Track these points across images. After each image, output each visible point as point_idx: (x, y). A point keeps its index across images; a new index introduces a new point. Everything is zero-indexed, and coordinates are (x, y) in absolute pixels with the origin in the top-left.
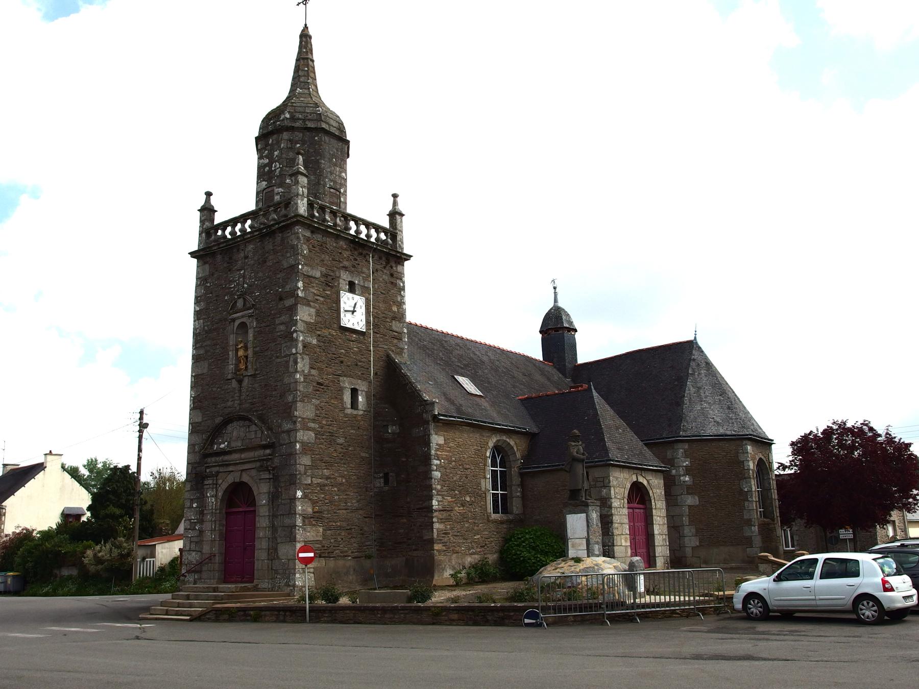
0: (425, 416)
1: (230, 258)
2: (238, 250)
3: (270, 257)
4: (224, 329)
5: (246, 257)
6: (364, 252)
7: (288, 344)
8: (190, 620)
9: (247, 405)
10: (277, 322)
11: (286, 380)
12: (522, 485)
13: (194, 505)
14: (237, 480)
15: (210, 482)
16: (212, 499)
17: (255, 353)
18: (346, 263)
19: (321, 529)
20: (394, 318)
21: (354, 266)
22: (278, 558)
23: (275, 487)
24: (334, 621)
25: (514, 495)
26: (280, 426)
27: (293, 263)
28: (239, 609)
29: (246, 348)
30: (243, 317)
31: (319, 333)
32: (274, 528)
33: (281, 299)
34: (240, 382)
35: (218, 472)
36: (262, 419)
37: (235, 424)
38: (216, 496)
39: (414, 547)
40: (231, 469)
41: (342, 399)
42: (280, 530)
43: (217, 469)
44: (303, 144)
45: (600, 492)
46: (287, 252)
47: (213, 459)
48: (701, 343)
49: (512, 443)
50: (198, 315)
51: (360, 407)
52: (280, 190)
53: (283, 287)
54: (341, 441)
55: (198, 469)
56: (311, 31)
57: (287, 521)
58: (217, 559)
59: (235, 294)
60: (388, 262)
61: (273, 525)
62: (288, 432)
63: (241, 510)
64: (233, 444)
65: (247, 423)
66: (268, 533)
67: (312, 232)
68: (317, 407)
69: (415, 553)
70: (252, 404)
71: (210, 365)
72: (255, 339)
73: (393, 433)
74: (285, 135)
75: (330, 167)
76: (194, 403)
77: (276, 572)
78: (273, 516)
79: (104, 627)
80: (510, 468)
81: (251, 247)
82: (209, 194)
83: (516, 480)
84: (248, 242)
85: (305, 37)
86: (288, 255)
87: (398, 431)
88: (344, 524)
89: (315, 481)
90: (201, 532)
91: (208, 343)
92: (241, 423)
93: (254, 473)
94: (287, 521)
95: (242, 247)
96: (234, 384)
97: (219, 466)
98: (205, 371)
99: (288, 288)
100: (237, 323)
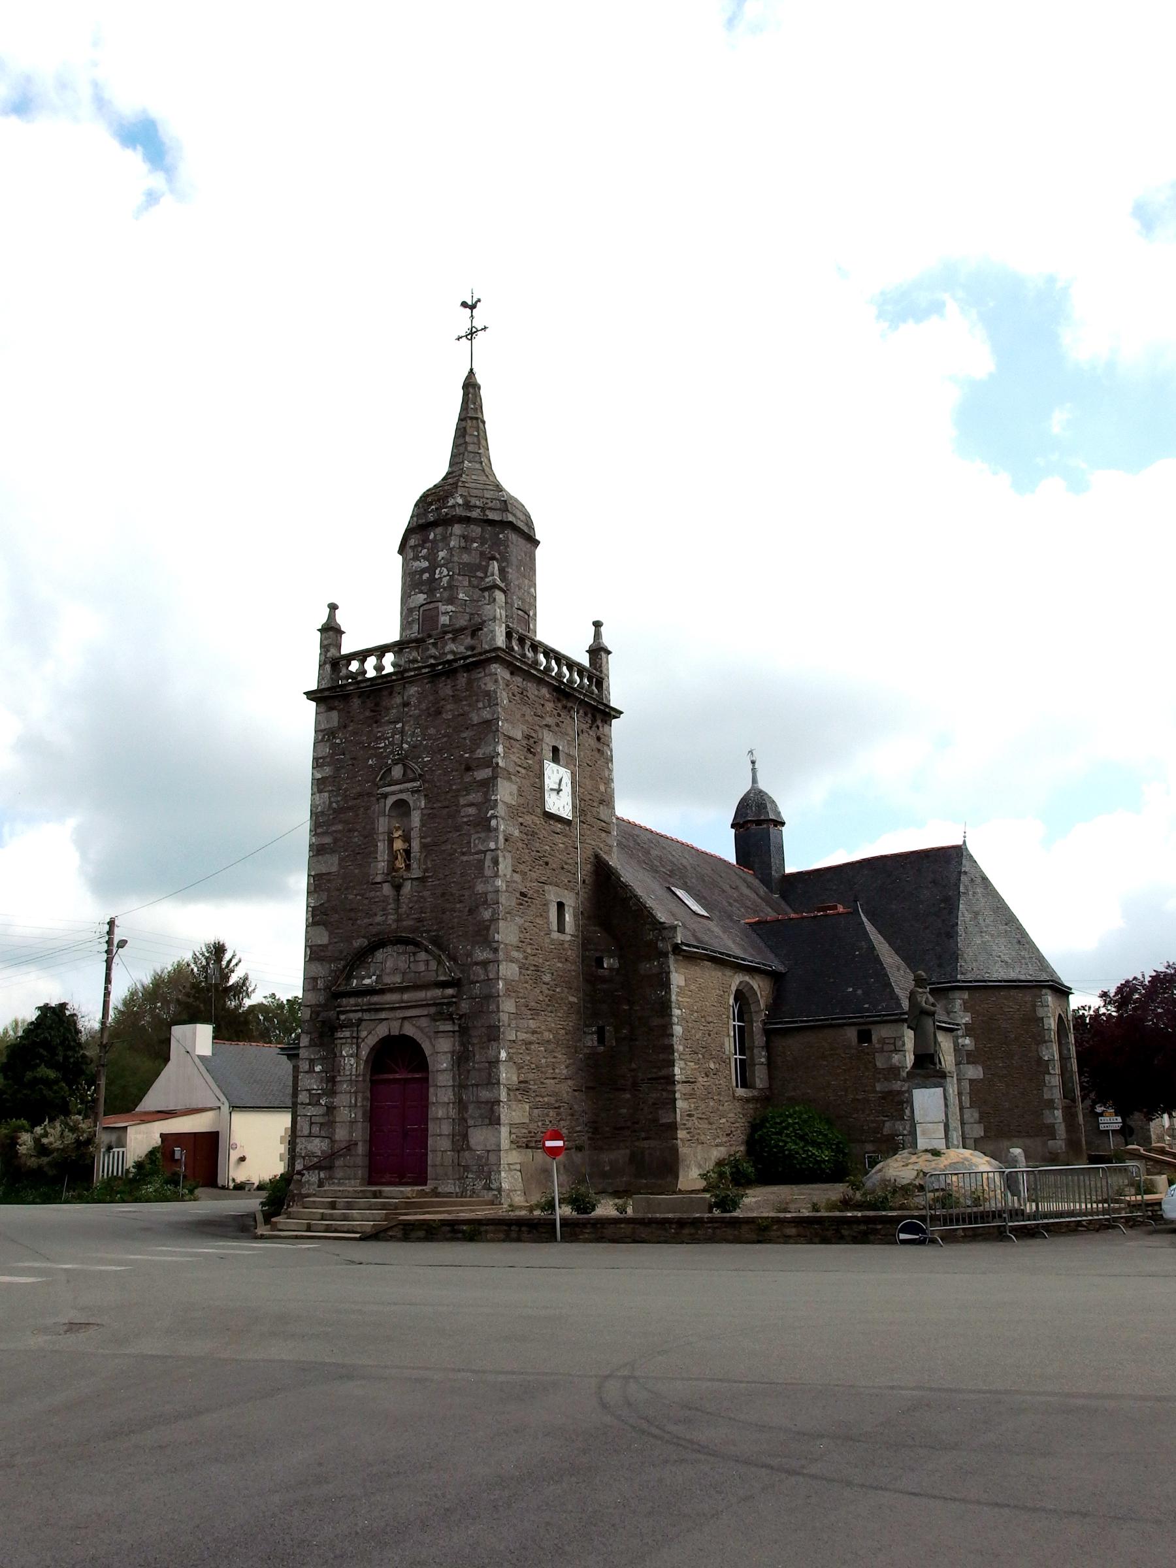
0: (660, 945)
1: (377, 705)
2: (391, 693)
3: (449, 707)
4: (367, 808)
5: (406, 704)
6: (570, 705)
7: (483, 835)
8: (360, 1239)
9: (411, 923)
10: (462, 801)
11: (480, 888)
12: (768, 1047)
13: (318, 1068)
14: (395, 1032)
15: (348, 1034)
16: (352, 1061)
17: (424, 846)
18: (549, 720)
19: (527, 1107)
20: (602, 802)
21: (557, 725)
22: (469, 1148)
23: (462, 1044)
24: (600, 1239)
25: (757, 1061)
26: (469, 954)
27: (489, 717)
28: (444, 1223)
29: (406, 838)
30: (401, 791)
31: (520, 820)
32: (461, 1105)
33: (468, 769)
34: (398, 888)
35: (360, 1020)
36: (436, 941)
37: (389, 949)
38: (357, 1056)
39: (643, 1135)
40: (383, 1015)
41: (547, 918)
42: (471, 1107)
43: (359, 1015)
44: (482, 544)
45: (890, 1058)
46: (477, 701)
47: (352, 1001)
48: (973, 849)
49: (756, 987)
50: (319, 785)
51: (567, 929)
52: (450, 608)
53: (472, 752)
54: (547, 978)
55: (324, 1015)
56: (480, 379)
57: (485, 1094)
58: (361, 1149)
59: (387, 757)
60: (594, 720)
61: (461, 1100)
62: (485, 964)
63: (397, 1076)
64: (387, 980)
65: (411, 948)
66: (453, 1113)
67: (512, 673)
68: (523, 930)
69: (646, 1144)
70: (420, 920)
71: (341, 860)
72: (423, 825)
73: (611, 969)
74: (457, 529)
75: (518, 578)
76: (313, 916)
77: (467, 1168)
78: (460, 1086)
80: (751, 1022)
81: (413, 690)
82: (333, 607)
83: (759, 1039)
84: (410, 682)
85: (471, 387)
86: (480, 705)
87: (617, 966)
88: (552, 1100)
89: (522, 1036)
90: (331, 1109)
91: (340, 827)
92: (401, 948)
93: (424, 1022)
94: (485, 1094)
95: (398, 689)
96: (387, 889)
97: (362, 1011)
98: (334, 869)
99: (480, 753)
100: (390, 800)
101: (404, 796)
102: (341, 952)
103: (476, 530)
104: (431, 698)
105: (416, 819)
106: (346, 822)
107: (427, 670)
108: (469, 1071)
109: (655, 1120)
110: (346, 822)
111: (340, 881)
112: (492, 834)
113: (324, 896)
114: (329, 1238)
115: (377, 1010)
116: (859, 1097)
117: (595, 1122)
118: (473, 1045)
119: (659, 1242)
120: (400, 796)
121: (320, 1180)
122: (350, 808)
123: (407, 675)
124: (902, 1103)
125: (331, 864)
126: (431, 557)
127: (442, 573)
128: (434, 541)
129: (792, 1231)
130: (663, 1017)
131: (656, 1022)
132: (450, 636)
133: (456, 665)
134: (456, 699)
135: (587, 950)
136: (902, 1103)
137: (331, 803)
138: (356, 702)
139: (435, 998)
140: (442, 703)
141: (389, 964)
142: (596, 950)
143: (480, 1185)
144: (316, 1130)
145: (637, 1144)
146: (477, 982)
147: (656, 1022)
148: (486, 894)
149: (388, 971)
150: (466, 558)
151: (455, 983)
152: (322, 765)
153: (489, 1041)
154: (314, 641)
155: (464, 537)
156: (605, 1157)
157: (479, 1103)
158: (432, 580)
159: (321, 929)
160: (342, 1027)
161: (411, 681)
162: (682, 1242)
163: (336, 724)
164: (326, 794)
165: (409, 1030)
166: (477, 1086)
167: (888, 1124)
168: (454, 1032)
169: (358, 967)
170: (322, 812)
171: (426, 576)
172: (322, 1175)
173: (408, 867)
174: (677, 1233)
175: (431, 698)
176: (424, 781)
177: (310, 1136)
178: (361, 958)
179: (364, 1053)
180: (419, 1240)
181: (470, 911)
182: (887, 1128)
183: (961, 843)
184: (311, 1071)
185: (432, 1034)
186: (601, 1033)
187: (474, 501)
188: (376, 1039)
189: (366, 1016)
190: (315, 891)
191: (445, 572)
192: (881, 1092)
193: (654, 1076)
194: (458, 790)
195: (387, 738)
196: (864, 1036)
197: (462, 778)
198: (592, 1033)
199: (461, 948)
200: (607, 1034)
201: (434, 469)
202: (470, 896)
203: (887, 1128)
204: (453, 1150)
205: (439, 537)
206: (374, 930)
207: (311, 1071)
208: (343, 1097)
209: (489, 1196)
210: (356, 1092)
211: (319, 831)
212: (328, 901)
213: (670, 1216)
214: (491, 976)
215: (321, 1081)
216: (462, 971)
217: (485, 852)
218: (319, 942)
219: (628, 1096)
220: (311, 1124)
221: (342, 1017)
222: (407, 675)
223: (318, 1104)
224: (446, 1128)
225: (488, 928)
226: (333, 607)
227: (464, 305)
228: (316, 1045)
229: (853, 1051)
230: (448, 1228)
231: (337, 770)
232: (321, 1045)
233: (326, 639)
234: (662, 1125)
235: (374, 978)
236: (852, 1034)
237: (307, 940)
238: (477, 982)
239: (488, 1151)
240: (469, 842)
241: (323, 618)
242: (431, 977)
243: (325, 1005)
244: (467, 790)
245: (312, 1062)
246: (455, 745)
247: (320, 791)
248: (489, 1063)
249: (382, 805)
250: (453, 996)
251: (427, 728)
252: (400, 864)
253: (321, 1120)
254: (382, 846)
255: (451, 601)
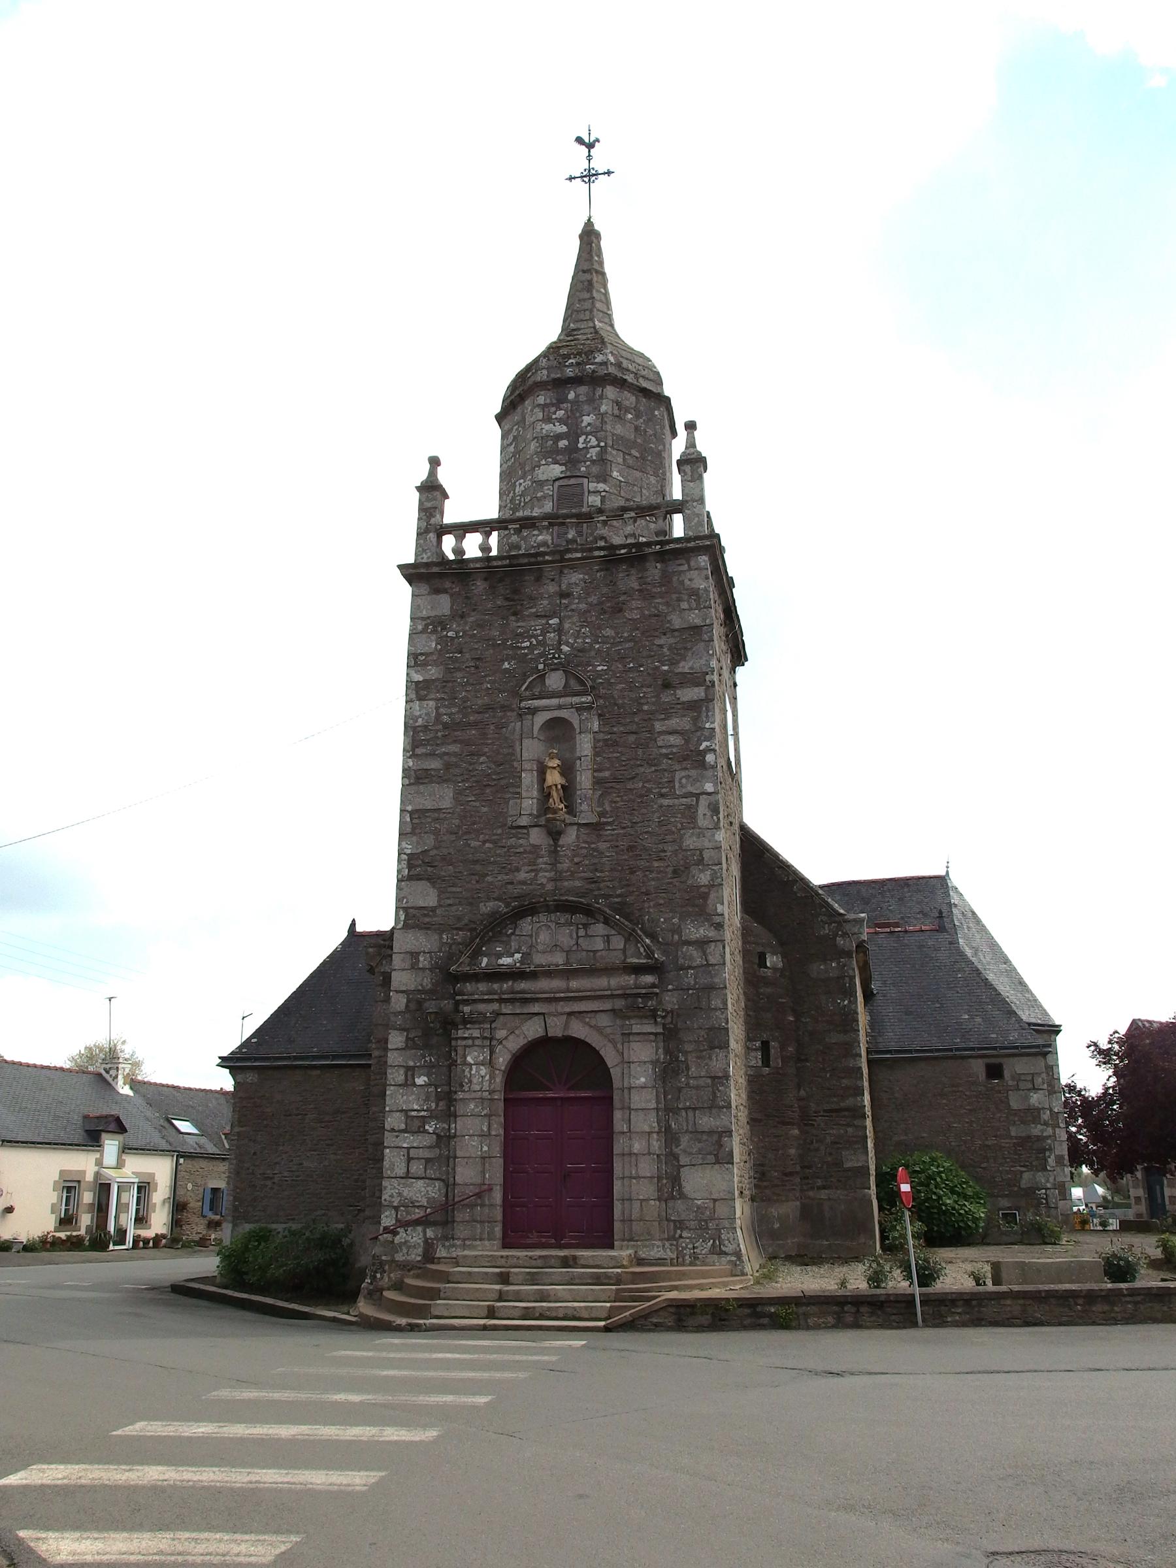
0: (840, 941)
1: (516, 591)
2: (538, 579)
3: (634, 604)
4: (500, 727)
5: (564, 595)
7: (693, 773)
8: (607, 1329)
9: (578, 884)
10: (658, 726)
11: (690, 842)
13: (421, 1080)
14: (556, 1031)
15: (476, 1033)
16: (482, 1071)
17: (597, 782)
22: (682, 1196)
23: (667, 1051)
24: (977, 1322)
26: (678, 930)
27: (698, 622)
28: (743, 1303)
29: (567, 770)
30: (560, 707)
32: (670, 1136)
33: (667, 686)
34: (555, 834)
35: (498, 1014)
36: (620, 909)
37: (543, 917)
38: (491, 1064)
39: (819, 1182)
40: (536, 1008)
42: (685, 1140)
43: (496, 1006)
44: (637, 416)
45: (1027, 1098)
46: (679, 600)
47: (482, 987)
48: (955, 880)
50: (417, 691)
52: (601, 486)
53: (673, 663)
55: (431, 1006)
57: (706, 1121)
58: (498, 1196)
59: (536, 660)
61: (668, 1128)
62: (702, 944)
63: (550, 1095)
64: (540, 959)
65: (580, 918)
66: (656, 1145)
69: (824, 1194)
70: (592, 881)
71: (458, 793)
72: (596, 754)
73: (775, 969)
74: (610, 392)
76: (410, 866)
77: (680, 1225)
78: (668, 1110)
79: (557, 1350)
81: (575, 577)
82: (435, 462)
84: (572, 567)
85: (590, 238)
86: (684, 605)
87: (780, 965)
90: (445, 1140)
91: (454, 748)
92: (563, 918)
93: (604, 1021)
94: (706, 1121)
95: (549, 571)
96: (537, 837)
97: (501, 1001)
98: (447, 803)
99: (684, 667)
100: (541, 719)
101: (563, 714)
102: (459, 919)
103: (629, 399)
104: (605, 590)
105: (585, 745)
106: (466, 743)
107: (602, 553)
108: (680, 1090)
109: (838, 1164)
110: (466, 743)
111: (457, 822)
112: (709, 773)
113: (430, 841)
114: (540, 1328)
115: (525, 1001)
116: (989, 1143)
117: (762, 1165)
118: (686, 1053)
119: (1060, 1324)
120: (557, 714)
121: (426, 1241)
122: (474, 724)
123: (568, 556)
124: (1044, 1150)
125: (443, 797)
126: (571, 420)
127: (589, 444)
128: (576, 402)
129: (1015, 1307)
130: (845, 1032)
131: (835, 1038)
132: (633, 514)
133: (648, 550)
134: (645, 594)
135: (749, 943)
136: (1044, 1150)
137: (438, 715)
138: (480, 586)
139: (622, 988)
140: (622, 598)
141: (544, 937)
142: (757, 944)
143: (704, 1248)
144: (417, 1168)
145: (811, 1193)
146: (690, 967)
147: (835, 1038)
148: (701, 851)
149: (540, 948)
150: (619, 430)
151: (654, 968)
152: (425, 664)
153: (712, 1048)
154: (413, 499)
155: (617, 403)
156: (774, 1211)
157: (696, 1133)
158: (573, 449)
159: (423, 885)
160: (467, 1021)
161: (573, 565)
162: (1094, 1323)
163: (447, 611)
164: (432, 703)
165: (578, 1030)
166: (695, 1109)
167: (1026, 1176)
168: (656, 1034)
169: (489, 940)
170: (425, 728)
171: (563, 443)
172: (430, 1233)
173: (571, 810)
174: (1083, 1311)
175: (605, 590)
176: (598, 697)
177: (407, 1176)
178: (497, 927)
179: (502, 1060)
180: (700, 1329)
181: (675, 872)
182: (1026, 1179)
183: (943, 873)
184: (408, 1083)
185: (618, 1038)
186: (765, 1047)
187: (625, 364)
188: (522, 1042)
189: (507, 1009)
190: (413, 833)
191: (594, 442)
192: (1016, 1138)
193: (834, 1106)
194: (652, 713)
195: (535, 637)
196: (995, 1071)
197: (658, 697)
198: (756, 1050)
199: (663, 920)
200: (772, 1051)
201: (542, 328)
202: (675, 852)
203: (1026, 1179)
204: (659, 1199)
205: (582, 398)
206: (517, 890)
207: (408, 1083)
208: (469, 1121)
209: (722, 1264)
210: (489, 1116)
211: (419, 751)
212: (436, 848)
213: (1074, 1287)
214: (712, 961)
215: (427, 1099)
216: (665, 953)
217: (697, 796)
218: (421, 904)
219: (796, 1132)
220: (409, 1159)
221: (467, 1009)
222: (568, 556)
223: (421, 1130)
224: (647, 1168)
225: (705, 897)
226: (435, 462)
227: (579, 140)
228: (416, 1047)
229: (981, 1088)
230: (747, 1311)
231: (448, 671)
232: (427, 1046)
233: (428, 500)
234: (849, 1169)
235: (518, 956)
236: (978, 1068)
237: (399, 900)
238: (690, 967)
239: (715, 1200)
240: (672, 781)
241: (422, 474)
242: (616, 958)
243: (431, 992)
244: (667, 712)
245: (410, 1071)
246: (645, 653)
247: (421, 698)
248: (713, 1078)
249: (527, 723)
250: (653, 986)
251: (600, 628)
252: (556, 801)
253: (427, 1154)
254: (528, 779)
255: (603, 477)
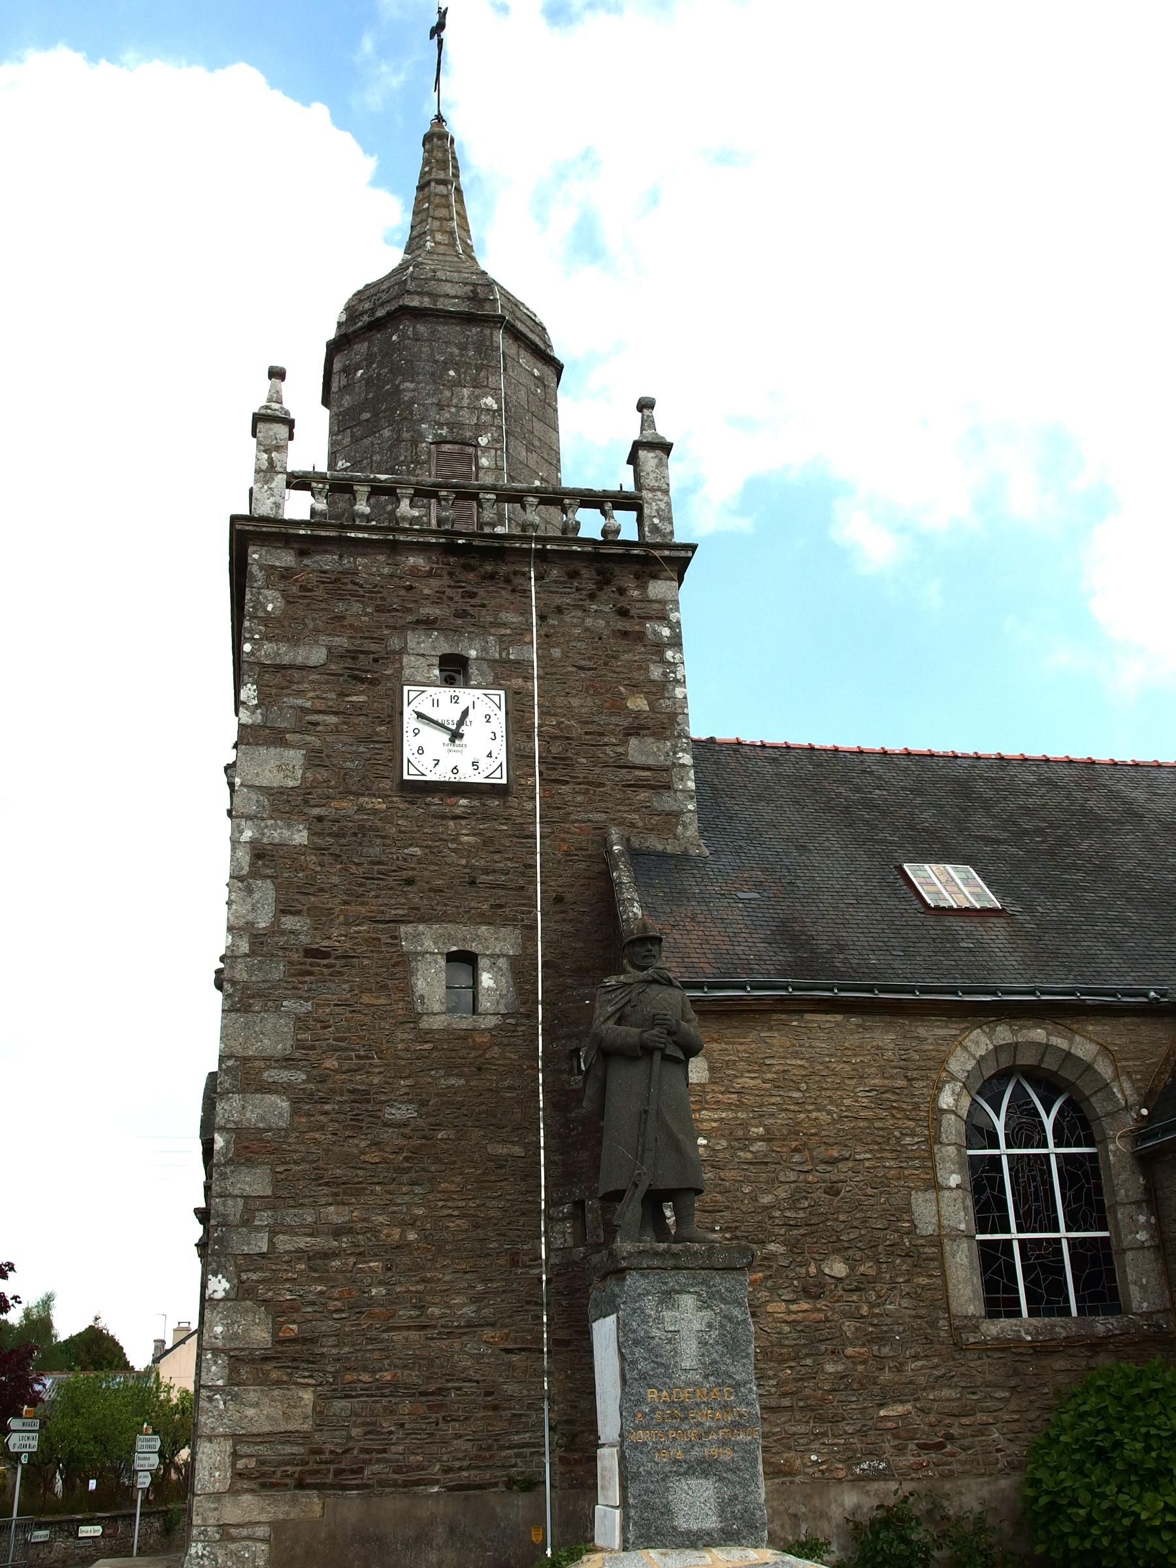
6: (504, 569)
12: (1152, 1200)
18: (429, 611)
19: (308, 1396)
20: (637, 728)
21: (462, 614)
25: (1127, 1240)
31: (316, 811)
41: (407, 990)
49: (1084, 1049)
51: (485, 1004)
54: (402, 1112)
56: (455, 127)
60: (604, 580)
67: (302, 553)
68: (301, 1022)
75: (437, 391)
80: (1104, 1141)
83: (1123, 1184)
88: (412, 1377)
89: (285, 1243)
198: (563, 1220)
